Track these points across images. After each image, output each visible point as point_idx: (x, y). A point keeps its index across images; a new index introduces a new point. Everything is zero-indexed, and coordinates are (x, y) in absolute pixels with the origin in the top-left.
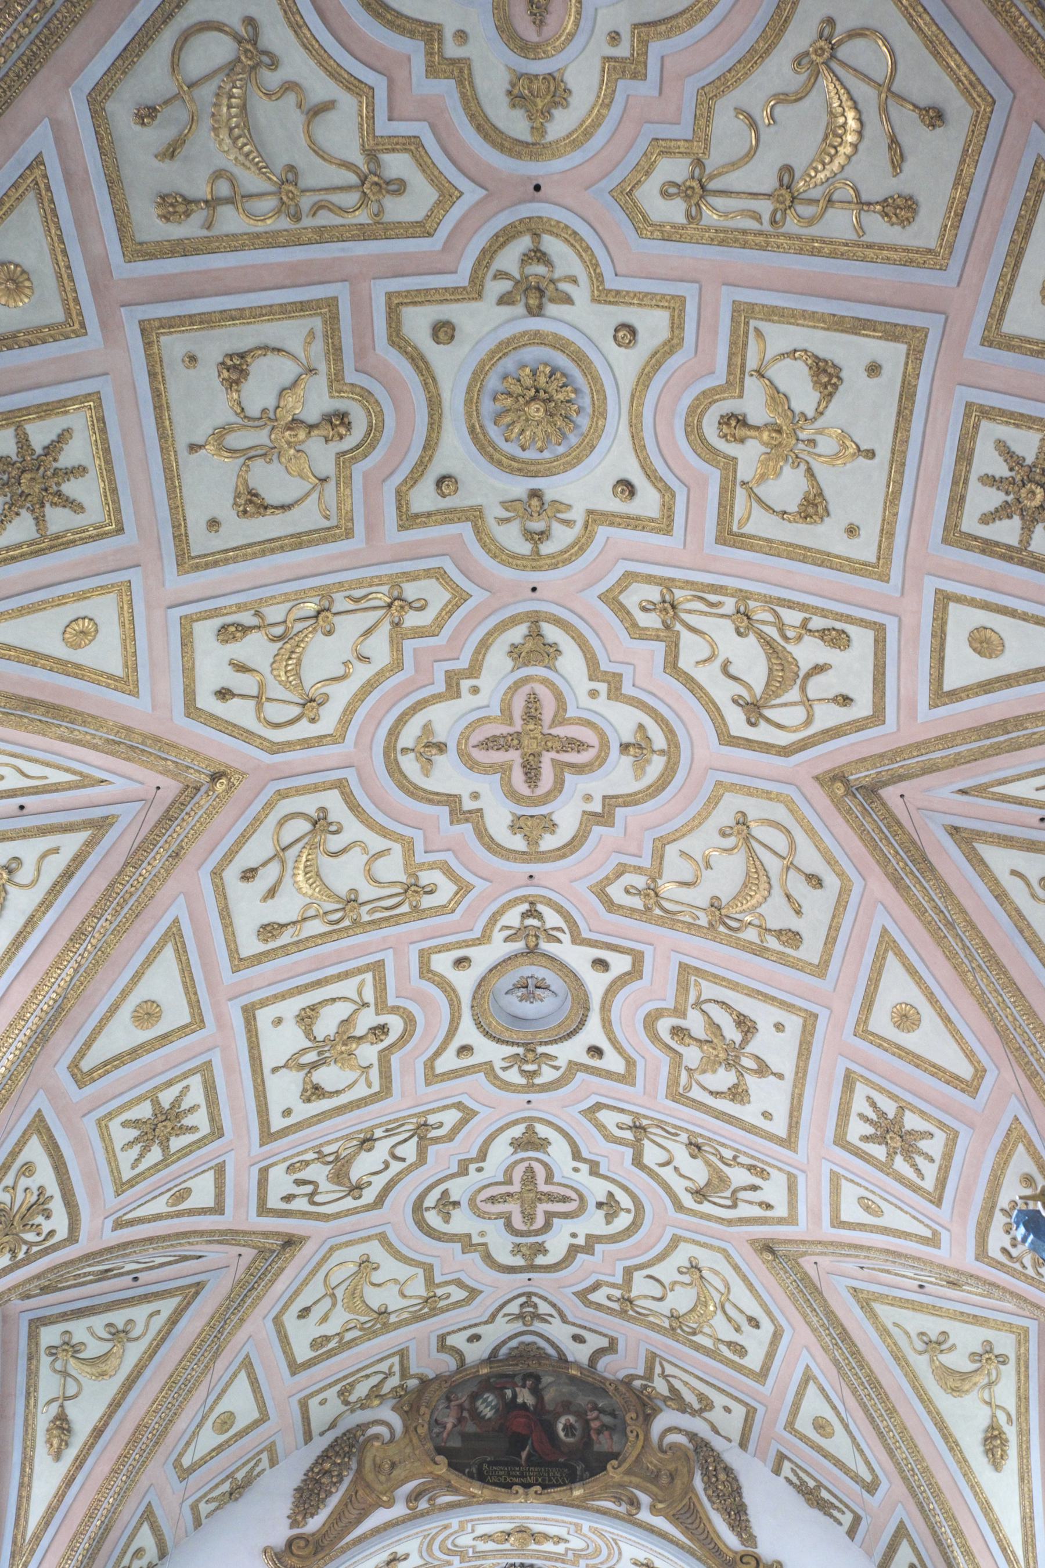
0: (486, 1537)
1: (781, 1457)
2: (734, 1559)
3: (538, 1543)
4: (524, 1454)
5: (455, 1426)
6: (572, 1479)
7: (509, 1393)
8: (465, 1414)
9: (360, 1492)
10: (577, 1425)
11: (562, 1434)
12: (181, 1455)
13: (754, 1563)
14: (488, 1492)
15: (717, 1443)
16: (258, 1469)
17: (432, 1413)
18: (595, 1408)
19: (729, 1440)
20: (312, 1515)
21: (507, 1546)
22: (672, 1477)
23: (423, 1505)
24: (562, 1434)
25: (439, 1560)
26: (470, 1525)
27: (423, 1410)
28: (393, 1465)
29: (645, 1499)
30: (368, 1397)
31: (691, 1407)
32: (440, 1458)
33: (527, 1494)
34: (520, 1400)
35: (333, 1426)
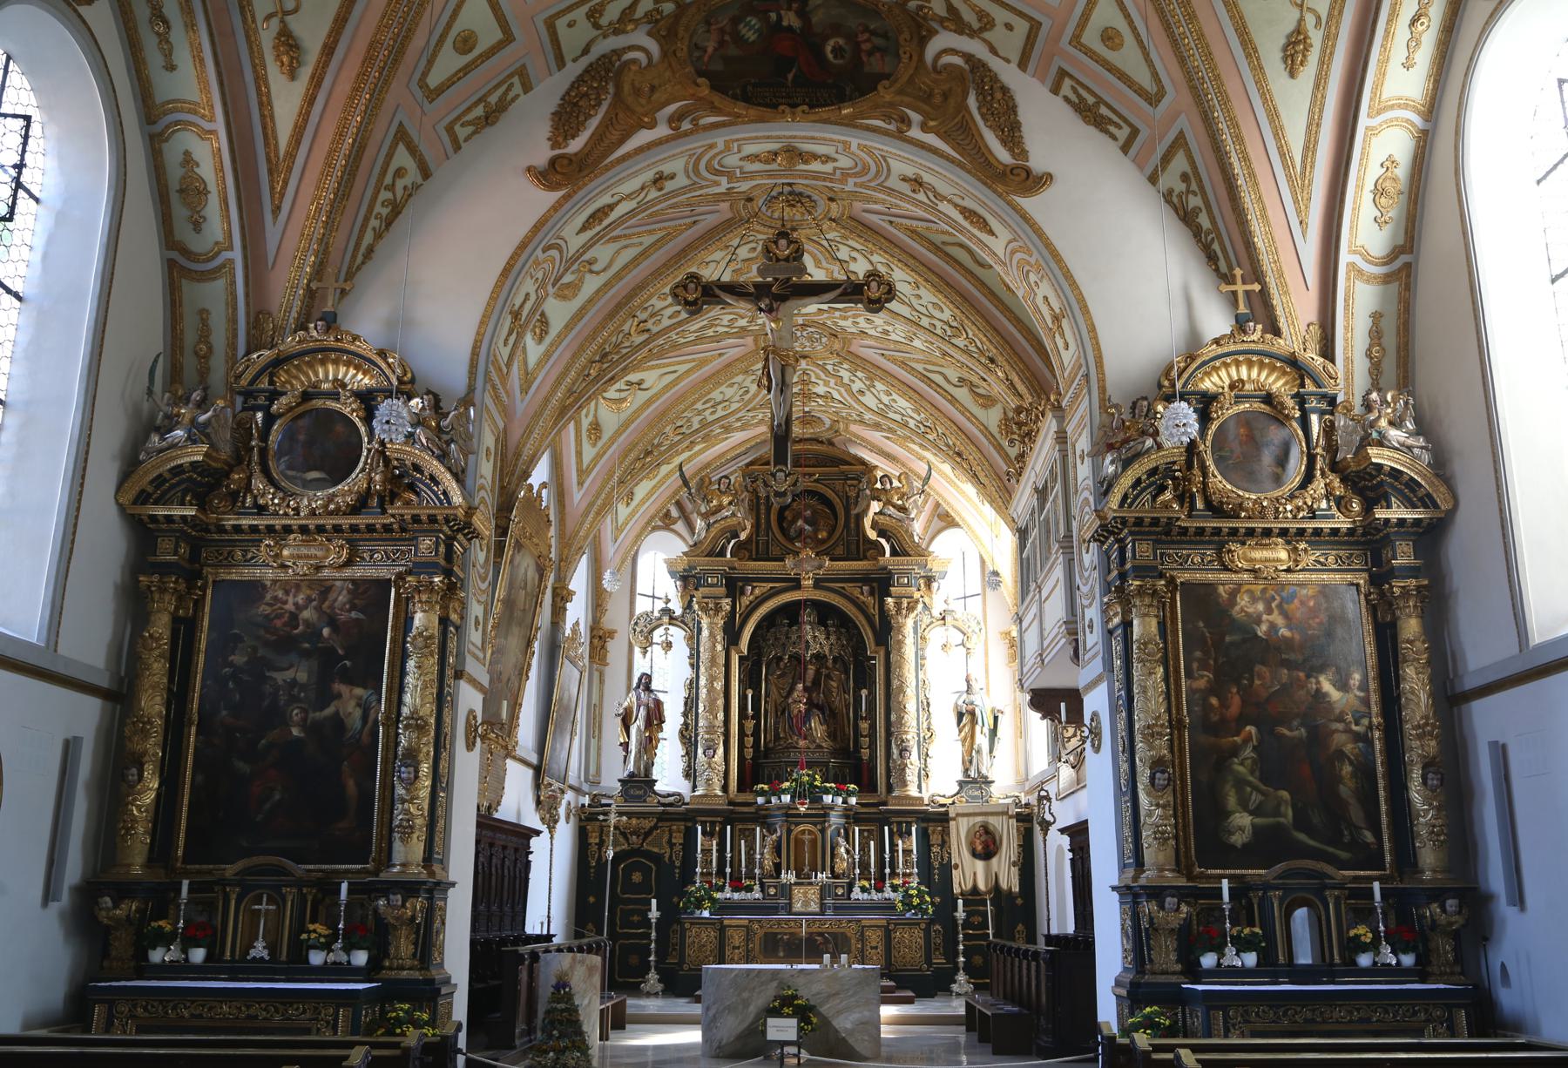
0: (754, 158)
1: (1062, 74)
2: (1004, 171)
3: (806, 162)
4: (790, 76)
5: (716, 50)
6: (840, 98)
7: (773, 16)
8: (727, 38)
9: (621, 115)
10: (846, 47)
11: (830, 56)
12: (425, 74)
13: (1024, 175)
14: (753, 112)
15: (995, 64)
16: (511, 95)
17: (691, 37)
18: (866, 29)
19: (1008, 61)
20: (573, 137)
21: (774, 166)
22: (945, 96)
23: (686, 125)
24: (830, 56)
26: (735, 145)
27: (680, 36)
28: (653, 89)
29: (915, 117)
30: (620, 20)
31: (970, 27)
32: (700, 80)
33: (794, 114)
34: (785, 23)
35: (586, 51)
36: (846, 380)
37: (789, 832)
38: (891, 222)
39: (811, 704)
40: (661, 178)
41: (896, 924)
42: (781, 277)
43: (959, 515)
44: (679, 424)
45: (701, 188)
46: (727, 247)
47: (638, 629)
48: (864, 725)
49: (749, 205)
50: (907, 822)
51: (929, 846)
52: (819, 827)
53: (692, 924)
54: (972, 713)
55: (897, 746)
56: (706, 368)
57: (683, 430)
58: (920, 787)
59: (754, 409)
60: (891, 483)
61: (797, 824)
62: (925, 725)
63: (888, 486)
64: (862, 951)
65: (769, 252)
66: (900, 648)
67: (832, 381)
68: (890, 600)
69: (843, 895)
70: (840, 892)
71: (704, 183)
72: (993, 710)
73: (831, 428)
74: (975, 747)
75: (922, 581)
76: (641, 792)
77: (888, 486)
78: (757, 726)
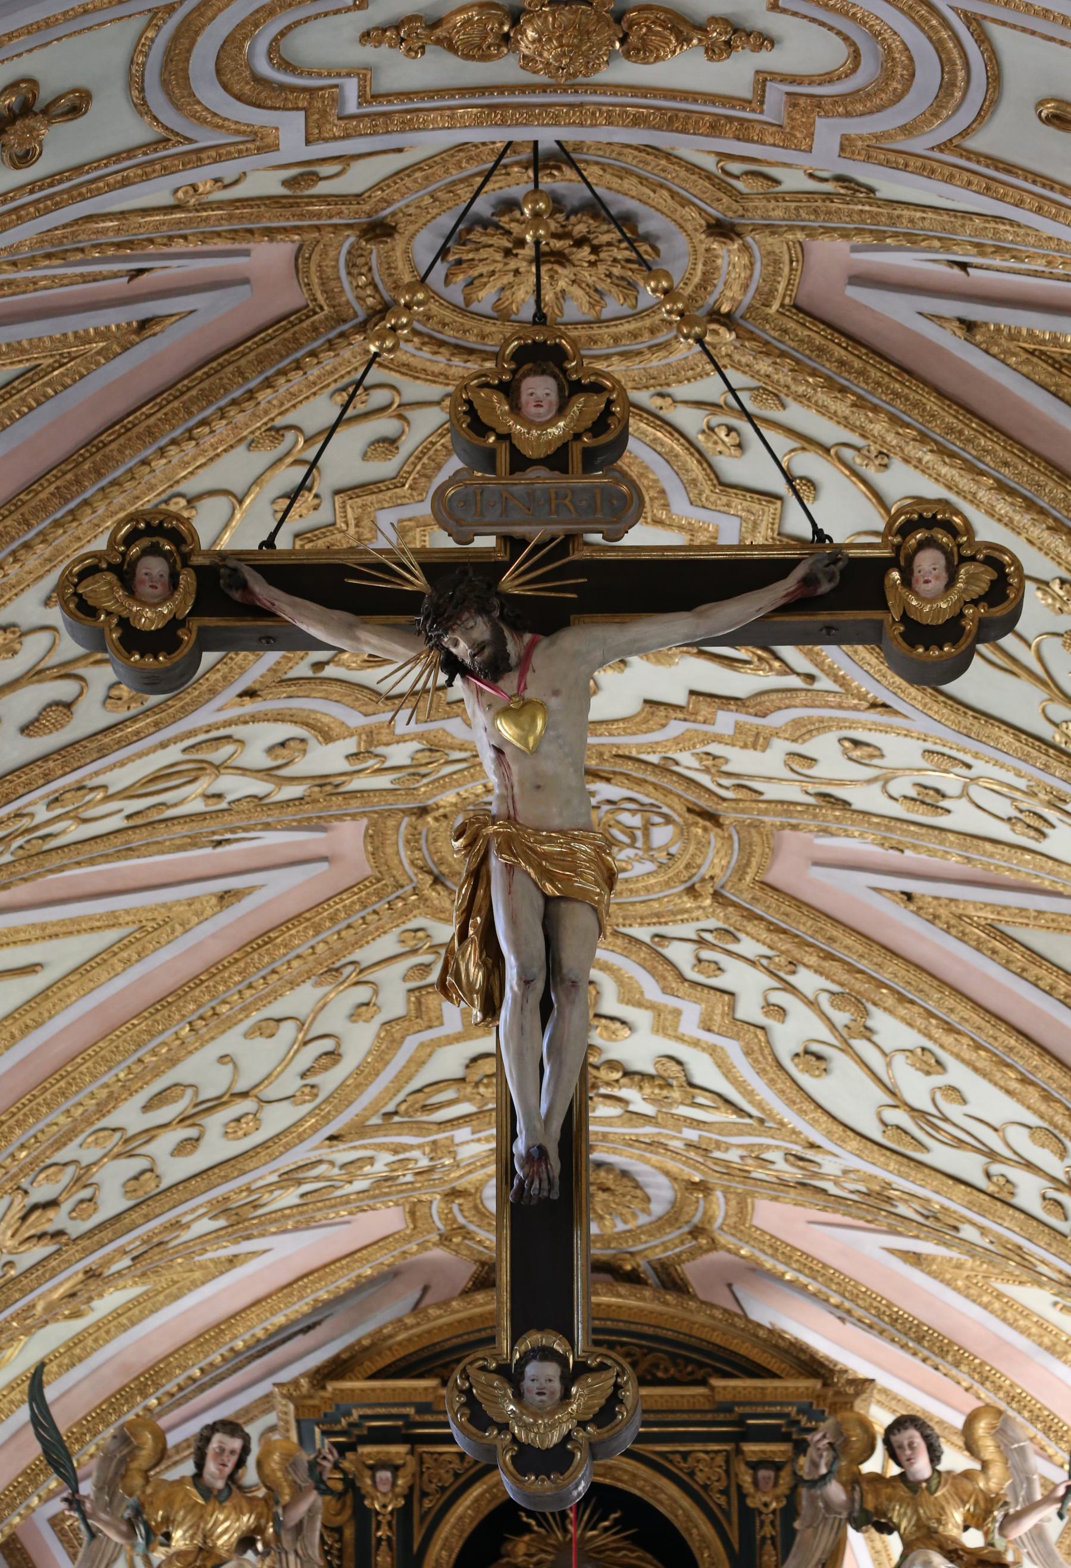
25: (217, 123)
36: (749, 1009)
38: (969, 326)
40: (26, 109)
42: (536, 533)
44: (41, 1192)
45: (197, 158)
46: (277, 432)
49: (375, 251)
56: (164, 955)
57: (58, 1219)
59: (360, 1129)
60: (935, 1456)
63: (922, 1467)
65: (479, 428)
67: (691, 1013)
71: (206, 138)
73: (673, 1216)
77: (922, 1467)
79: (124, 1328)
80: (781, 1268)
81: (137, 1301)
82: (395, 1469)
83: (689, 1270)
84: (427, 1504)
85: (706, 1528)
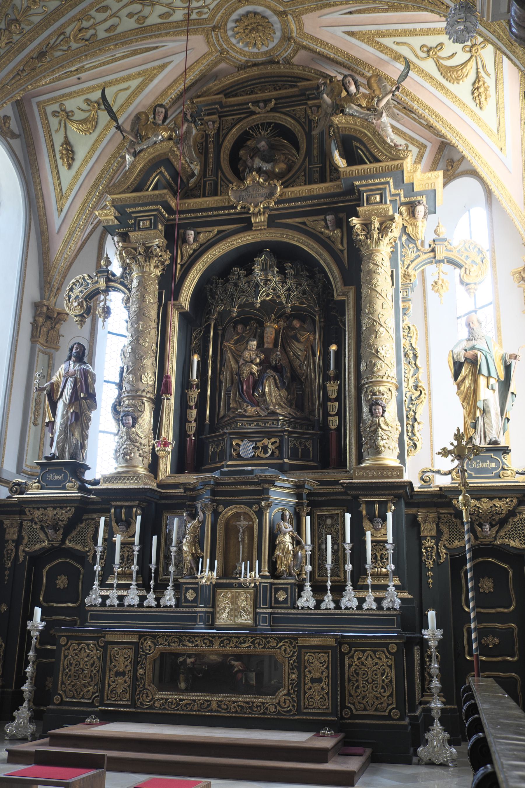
37: (216, 514)
39: (265, 365)
41: (351, 645)
43: (451, 128)
47: (73, 296)
48: (332, 387)
50: (380, 503)
51: (420, 539)
52: (255, 507)
53: (69, 638)
54: (473, 362)
55: (367, 401)
58: (401, 457)
61: (226, 505)
62: (411, 383)
64: (299, 685)
66: (371, 279)
68: (355, 221)
69: (285, 601)
70: (282, 597)
72: (503, 358)
74: (480, 404)
75: (403, 209)
76: (60, 477)
78: (202, 397)
79: (140, 92)
80: (316, 47)
81: (141, 83)
82: (214, 122)
83: (295, 60)
84: (224, 132)
85: (299, 127)
